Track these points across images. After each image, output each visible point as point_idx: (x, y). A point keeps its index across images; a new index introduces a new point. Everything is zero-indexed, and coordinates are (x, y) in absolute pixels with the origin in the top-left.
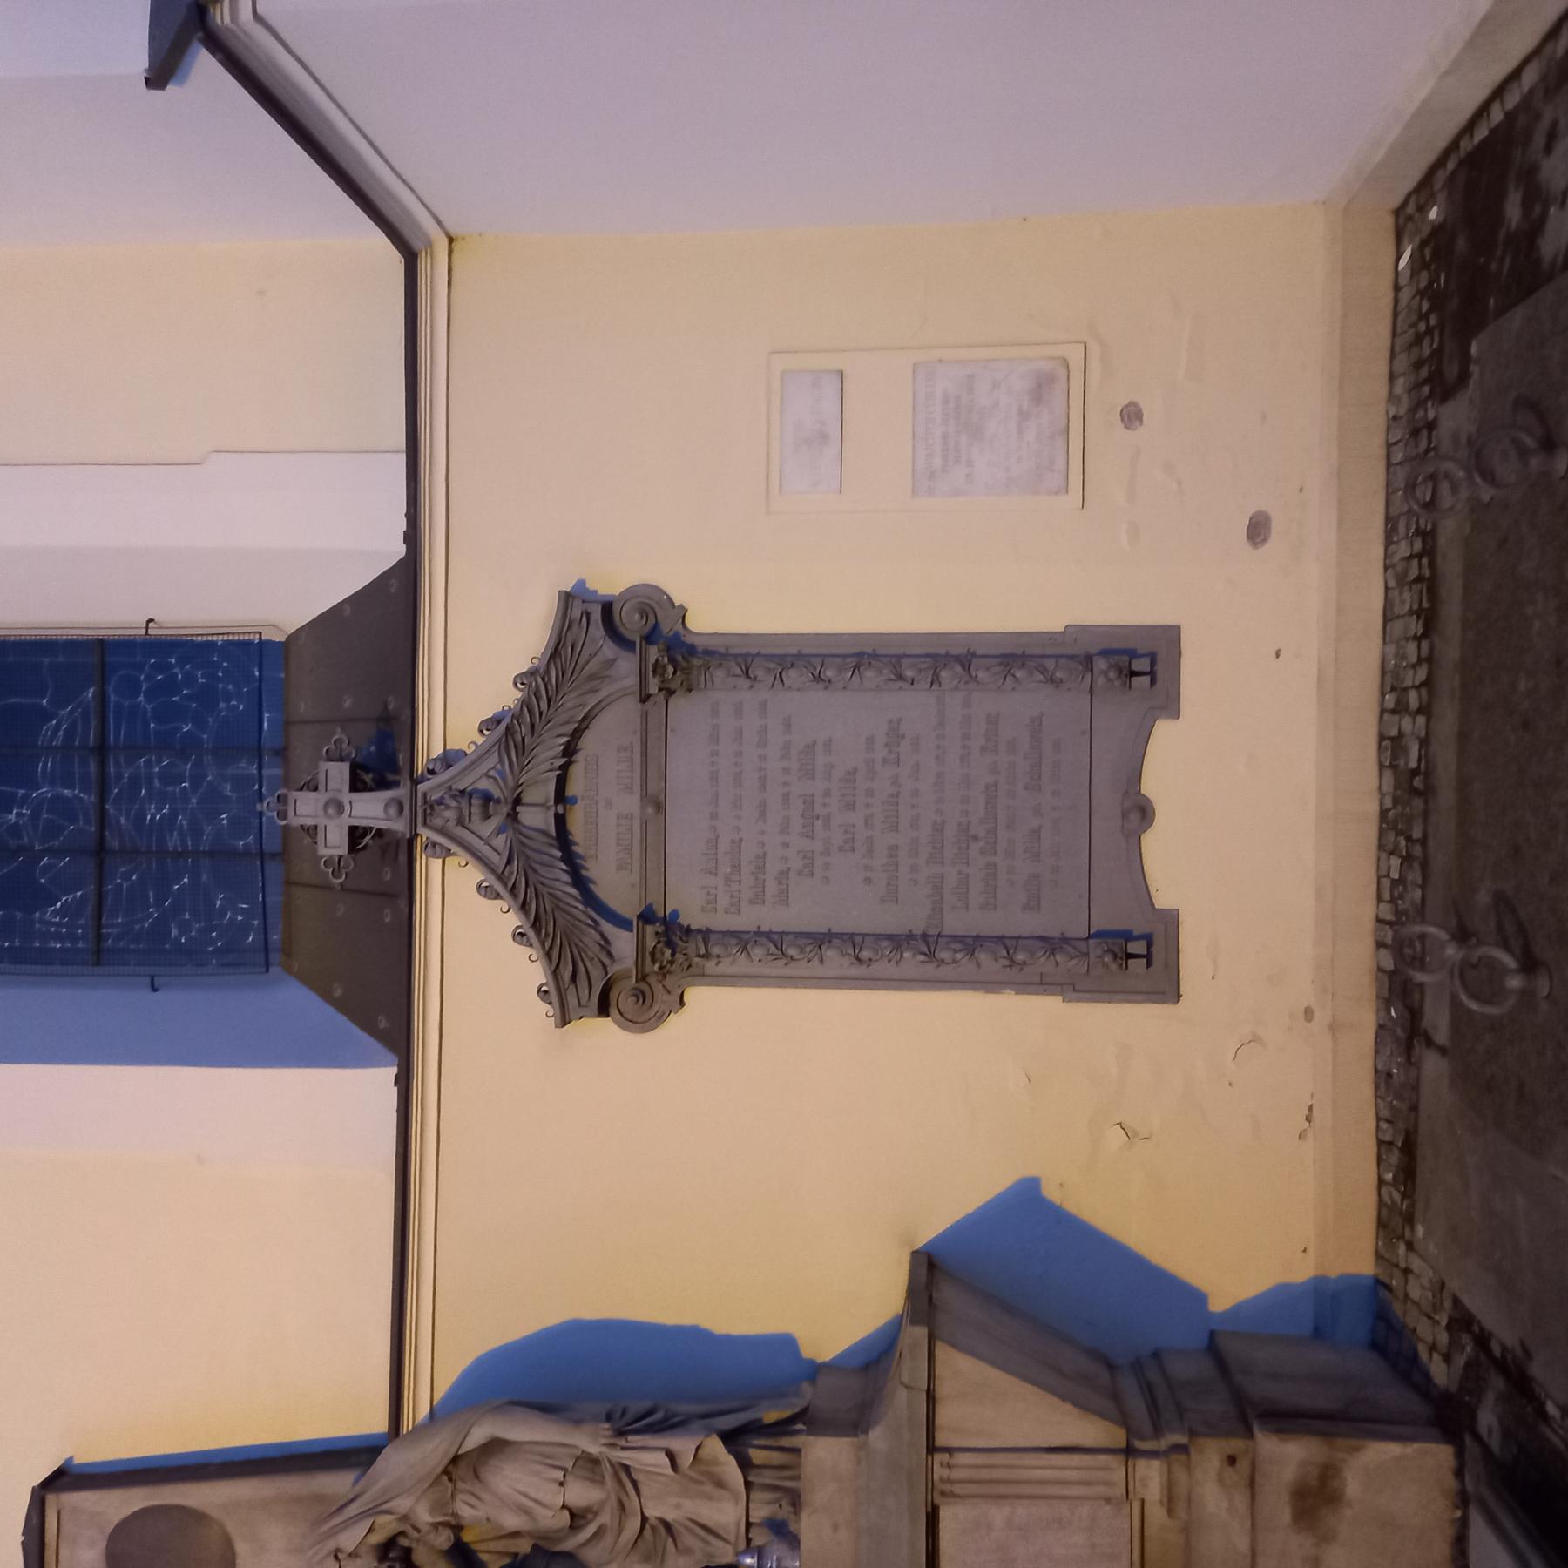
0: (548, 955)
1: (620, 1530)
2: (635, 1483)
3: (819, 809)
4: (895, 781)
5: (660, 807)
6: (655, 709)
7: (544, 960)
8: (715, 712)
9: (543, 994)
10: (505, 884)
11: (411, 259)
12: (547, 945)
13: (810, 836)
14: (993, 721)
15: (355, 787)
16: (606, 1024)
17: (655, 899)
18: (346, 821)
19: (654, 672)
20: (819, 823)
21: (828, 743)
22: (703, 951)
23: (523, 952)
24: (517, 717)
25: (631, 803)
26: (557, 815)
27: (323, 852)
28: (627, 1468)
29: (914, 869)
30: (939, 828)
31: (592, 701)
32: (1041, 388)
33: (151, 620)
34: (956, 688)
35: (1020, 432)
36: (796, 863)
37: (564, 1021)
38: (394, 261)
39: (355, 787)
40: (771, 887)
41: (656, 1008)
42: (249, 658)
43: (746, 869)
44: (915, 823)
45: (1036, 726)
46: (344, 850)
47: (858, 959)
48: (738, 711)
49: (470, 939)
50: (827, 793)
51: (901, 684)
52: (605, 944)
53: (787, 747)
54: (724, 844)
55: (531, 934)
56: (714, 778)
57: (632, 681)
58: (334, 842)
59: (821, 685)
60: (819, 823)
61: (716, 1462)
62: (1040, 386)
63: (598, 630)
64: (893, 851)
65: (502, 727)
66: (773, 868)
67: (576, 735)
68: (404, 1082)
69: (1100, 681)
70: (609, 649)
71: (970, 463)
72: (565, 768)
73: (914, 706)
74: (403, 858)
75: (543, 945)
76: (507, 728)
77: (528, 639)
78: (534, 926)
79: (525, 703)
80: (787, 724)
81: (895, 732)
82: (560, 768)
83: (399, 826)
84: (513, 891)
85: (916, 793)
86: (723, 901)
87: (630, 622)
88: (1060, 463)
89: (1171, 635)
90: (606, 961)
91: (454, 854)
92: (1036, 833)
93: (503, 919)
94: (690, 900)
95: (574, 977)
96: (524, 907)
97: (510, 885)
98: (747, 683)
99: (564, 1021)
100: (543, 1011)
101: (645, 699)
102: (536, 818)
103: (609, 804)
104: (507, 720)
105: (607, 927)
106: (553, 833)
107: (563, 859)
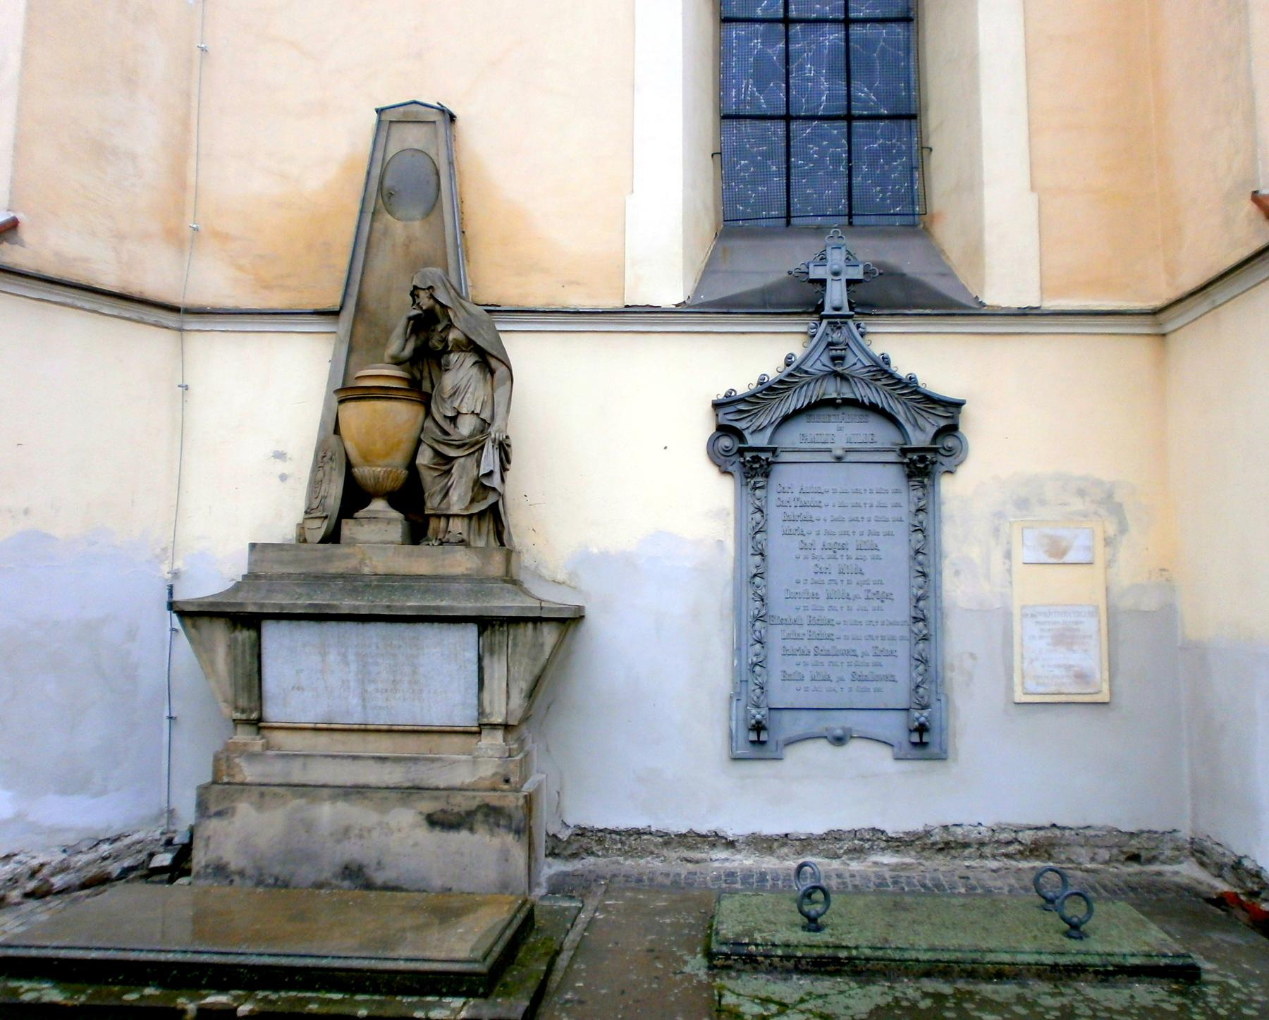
0: (754, 395)
1: (449, 445)
2: (473, 453)
3: (839, 553)
4: (857, 597)
5: (839, 459)
8: (897, 491)
11: (1155, 312)
13: (824, 548)
14: (892, 654)
16: (710, 429)
17: (785, 457)
18: (829, 278)
20: (831, 553)
23: (755, 382)
24: (891, 376)
28: (482, 448)
29: (806, 609)
30: (829, 623)
31: (902, 419)
35: (1059, 666)
36: (808, 540)
40: (793, 526)
42: (911, 214)
43: (804, 511)
44: (832, 608)
46: (812, 276)
47: (755, 575)
48: (897, 505)
54: (818, 497)
56: (857, 492)
57: (914, 444)
59: (912, 553)
60: (831, 553)
61: (485, 498)
63: (943, 423)
64: (816, 597)
65: (886, 367)
66: (806, 527)
69: (917, 714)
70: (932, 431)
71: (1041, 637)
73: (900, 609)
79: (900, 381)
83: (828, 310)
84: (790, 375)
85: (849, 609)
86: (785, 497)
87: (950, 442)
88: (1041, 690)
89: (941, 757)
90: (751, 430)
92: (828, 679)
94: (785, 477)
96: (781, 382)
98: (913, 509)
99: (717, 405)
102: (831, 390)
103: (840, 429)
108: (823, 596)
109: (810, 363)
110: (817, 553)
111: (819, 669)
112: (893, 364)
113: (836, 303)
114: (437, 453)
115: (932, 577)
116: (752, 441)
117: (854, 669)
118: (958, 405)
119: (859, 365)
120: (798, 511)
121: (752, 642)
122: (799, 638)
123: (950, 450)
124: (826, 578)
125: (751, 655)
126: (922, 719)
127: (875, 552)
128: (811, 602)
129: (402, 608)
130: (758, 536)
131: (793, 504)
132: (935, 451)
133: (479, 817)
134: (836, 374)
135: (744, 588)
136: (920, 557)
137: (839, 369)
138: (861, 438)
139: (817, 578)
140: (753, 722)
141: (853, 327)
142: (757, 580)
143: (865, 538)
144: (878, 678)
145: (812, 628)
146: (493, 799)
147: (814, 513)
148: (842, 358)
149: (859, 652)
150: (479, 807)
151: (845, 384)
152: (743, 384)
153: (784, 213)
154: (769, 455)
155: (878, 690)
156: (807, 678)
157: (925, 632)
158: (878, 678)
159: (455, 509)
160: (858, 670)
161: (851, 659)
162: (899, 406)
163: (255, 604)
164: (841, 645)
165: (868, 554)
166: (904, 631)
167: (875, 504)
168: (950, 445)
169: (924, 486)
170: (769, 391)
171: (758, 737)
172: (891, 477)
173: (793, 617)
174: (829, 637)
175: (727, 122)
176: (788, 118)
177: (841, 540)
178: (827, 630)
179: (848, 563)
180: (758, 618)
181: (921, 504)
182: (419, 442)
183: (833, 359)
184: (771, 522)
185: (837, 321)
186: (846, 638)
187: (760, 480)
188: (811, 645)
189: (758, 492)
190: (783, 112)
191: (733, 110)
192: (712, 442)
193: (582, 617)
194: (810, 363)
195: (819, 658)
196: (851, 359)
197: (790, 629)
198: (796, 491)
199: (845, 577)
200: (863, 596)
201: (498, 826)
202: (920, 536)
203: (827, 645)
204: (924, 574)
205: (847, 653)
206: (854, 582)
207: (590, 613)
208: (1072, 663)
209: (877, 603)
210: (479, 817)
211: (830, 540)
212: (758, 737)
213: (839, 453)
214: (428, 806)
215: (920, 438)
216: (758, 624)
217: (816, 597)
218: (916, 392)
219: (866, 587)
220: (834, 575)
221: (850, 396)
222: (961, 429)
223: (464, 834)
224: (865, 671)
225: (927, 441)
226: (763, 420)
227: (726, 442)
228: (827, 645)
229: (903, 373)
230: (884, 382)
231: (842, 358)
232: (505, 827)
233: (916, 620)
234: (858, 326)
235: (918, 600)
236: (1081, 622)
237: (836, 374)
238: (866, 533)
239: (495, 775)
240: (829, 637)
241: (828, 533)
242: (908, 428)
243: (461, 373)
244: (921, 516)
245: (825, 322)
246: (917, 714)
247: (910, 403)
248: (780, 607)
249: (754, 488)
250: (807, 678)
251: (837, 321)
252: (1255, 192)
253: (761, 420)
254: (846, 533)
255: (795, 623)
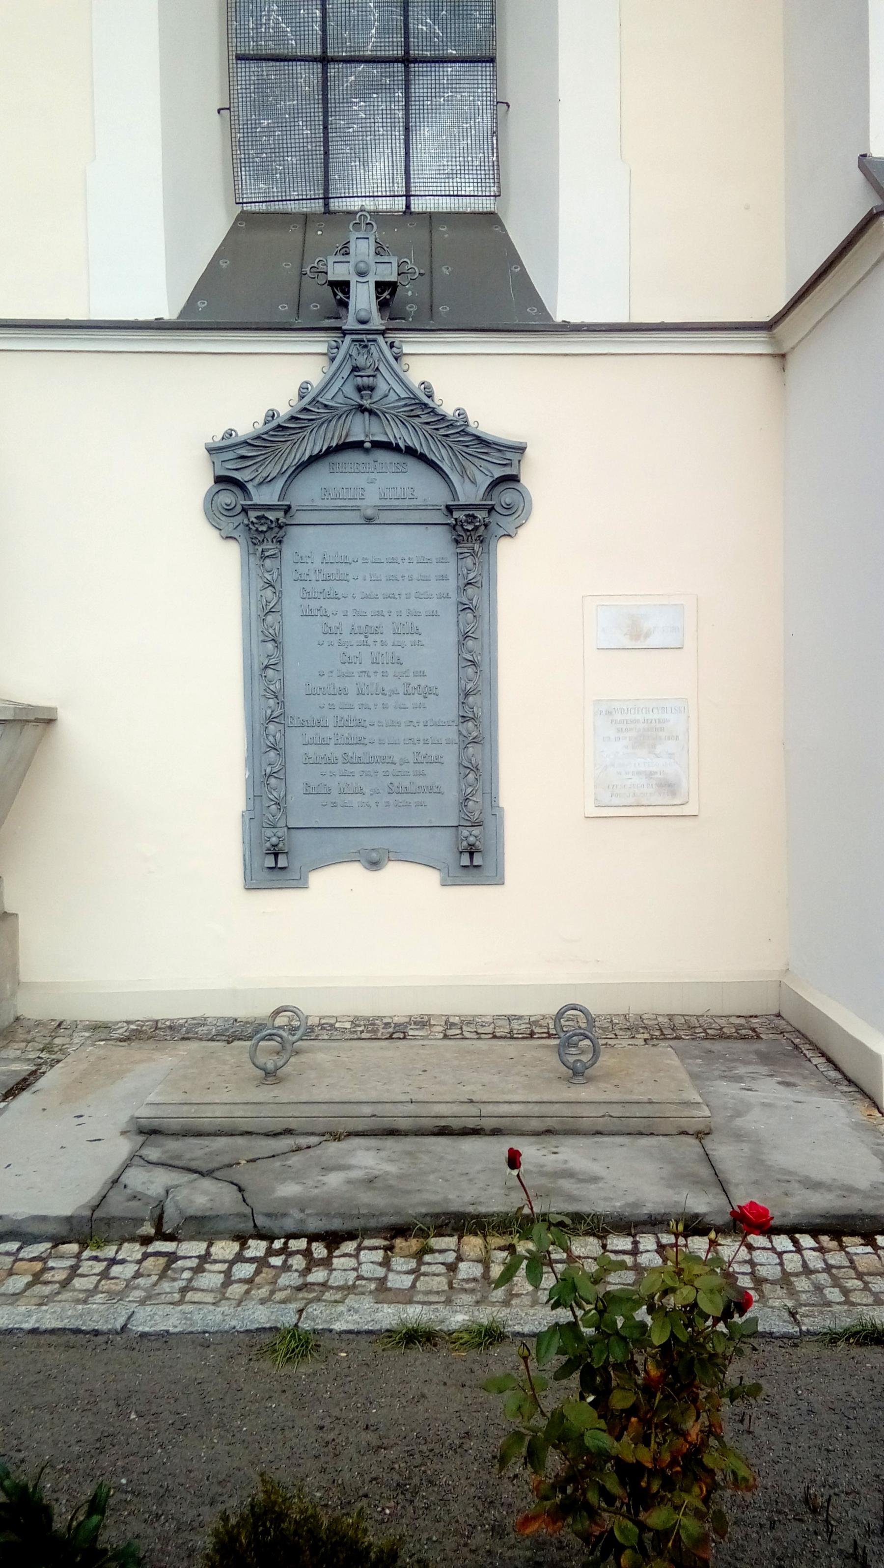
0: (258, 438)
3: (372, 638)
4: (394, 692)
5: (369, 521)
6: (439, 517)
7: (255, 434)
8: (442, 561)
9: (229, 434)
10: (310, 403)
11: (768, 326)
12: (264, 436)
14: (438, 761)
15: (378, 284)
16: (208, 482)
17: (301, 518)
18: (353, 279)
19: (468, 516)
20: (362, 638)
21: (419, 644)
22: (267, 554)
24: (433, 411)
25: (371, 500)
26: (363, 442)
27: (331, 260)
30: (360, 724)
32: (669, 787)
33: (508, 105)
34: (460, 733)
35: (639, 773)
36: (333, 622)
37: (212, 450)
38: (765, 314)
39: (378, 284)
40: (314, 604)
41: (223, 518)
43: (327, 585)
45: (435, 790)
46: (331, 277)
47: (266, 667)
48: (443, 578)
49: (267, 379)
50: (383, 644)
51: (462, 696)
52: (267, 481)
53: (417, 614)
54: (344, 568)
55: (274, 424)
56: (393, 561)
58: (338, 272)
59: (462, 639)
60: (362, 638)
62: (670, 785)
63: (498, 473)
64: (343, 692)
65: (426, 400)
66: (330, 606)
67: (422, 458)
68: (158, 326)
69: (465, 833)
70: (484, 482)
72: (396, 449)
73: (447, 706)
74: (327, 323)
75: (266, 433)
76: (426, 405)
77: (489, 422)
78: (279, 426)
79: (443, 418)
80: (434, 614)
81: (428, 692)
82: (397, 444)
84: (305, 410)
85: (385, 707)
87: (507, 497)
88: (616, 801)
89: (498, 879)
91: (330, 365)
93: (284, 403)
94: (304, 542)
95: (243, 457)
96: (293, 419)
97: (308, 407)
98: (462, 582)
99: (212, 450)
100: (215, 433)
101: (450, 509)
102: (359, 429)
104: (431, 404)
105: (279, 484)
106: (348, 440)
107: (329, 448)
108: (352, 690)
109: (329, 395)
110: (346, 637)
111: (349, 780)
112: (437, 397)
113: (363, 315)
115: (485, 667)
117: (390, 779)
118: (521, 449)
119: (392, 396)
120: (322, 586)
121: (264, 749)
122: (324, 743)
123: (508, 507)
124: (355, 669)
125: (264, 766)
126: (472, 839)
127: (416, 637)
128: (337, 700)
130: (270, 618)
131: (313, 577)
132: (491, 509)
134: (362, 409)
135: (256, 682)
136: (470, 643)
137: (366, 403)
138: (399, 493)
139: (344, 668)
140: (268, 845)
141: (386, 349)
142: (270, 672)
143: (403, 619)
144: (421, 790)
145: (341, 731)
147: (340, 588)
148: (372, 389)
149: (396, 760)
151: (373, 418)
152: (247, 422)
153: (320, 193)
154: (280, 514)
155: (420, 804)
156: (335, 792)
157: (474, 734)
158: (421, 790)
160: (396, 781)
161: (384, 767)
162: (443, 451)
164: (376, 751)
165: (408, 639)
166: (451, 733)
167: (415, 576)
168: (508, 501)
169: (474, 554)
170: (279, 432)
171: (274, 861)
172: (436, 543)
173: (317, 717)
174: (360, 742)
175: (242, 64)
176: (324, 60)
177: (375, 622)
178: (360, 732)
179: (383, 650)
180: (270, 720)
181: (471, 576)
183: (359, 389)
184: (286, 601)
185: (364, 338)
186: (381, 743)
187: (270, 547)
188: (338, 751)
189: (268, 562)
190: (317, 51)
191: (250, 48)
192: (211, 499)
193: (50, 721)
194: (329, 395)
195: (349, 768)
196: (382, 387)
197: (311, 732)
198: (318, 560)
199: (379, 668)
200: (401, 690)
202: (470, 616)
203: (359, 750)
204: (473, 663)
205: (383, 760)
206: (391, 674)
207: (63, 716)
208: (654, 769)
209: (418, 699)
211: (362, 622)
212: (274, 861)
213: (369, 512)
215: (470, 492)
216: (272, 727)
217: (343, 692)
218: (464, 433)
219: (404, 679)
220: (367, 666)
221: (383, 438)
222: (523, 480)
224: (405, 782)
225: (480, 498)
226: (272, 470)
227: (227, 498)
228: (359, 750)
229: (448, 409)
230: (425, 418)
231: (372, 389)
233: (464, 719)
234: (392, 346)
235: (467, 695)
236: (665, 721)
237: (362, 409)
238: (404, 613)
240: (360, 742)
241: (358, 613)
242: (455, 478)
244: (470, 590)
245: (348, 338)
246: (465, 833)
247: (456, 447)
248: (299, 706)
249: (264, 558)
250: (335, 792)
251: (364, 338)
252: (864, 156)
253: (269, 469)
254: (380, 614)
255: (319, 724)
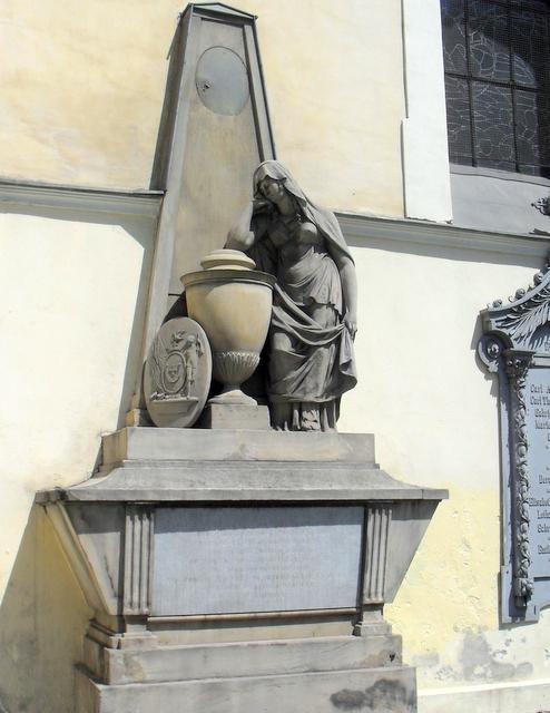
86: (536, 396)
95: (508, 320)
114: (296, 342)
116: (517, 347)
129: (302, 492)
133: (378, 692)
146: (388, 671)
150: (377, 684)
159: (310, 398)
163: (154, 491)
182: (273, 330)
201: (395, 699)
210: (378, 692)
214: (334, 687)
223: (366, 709)
232: (400, 699)
239: (381, 653)
243: (312, 264)
